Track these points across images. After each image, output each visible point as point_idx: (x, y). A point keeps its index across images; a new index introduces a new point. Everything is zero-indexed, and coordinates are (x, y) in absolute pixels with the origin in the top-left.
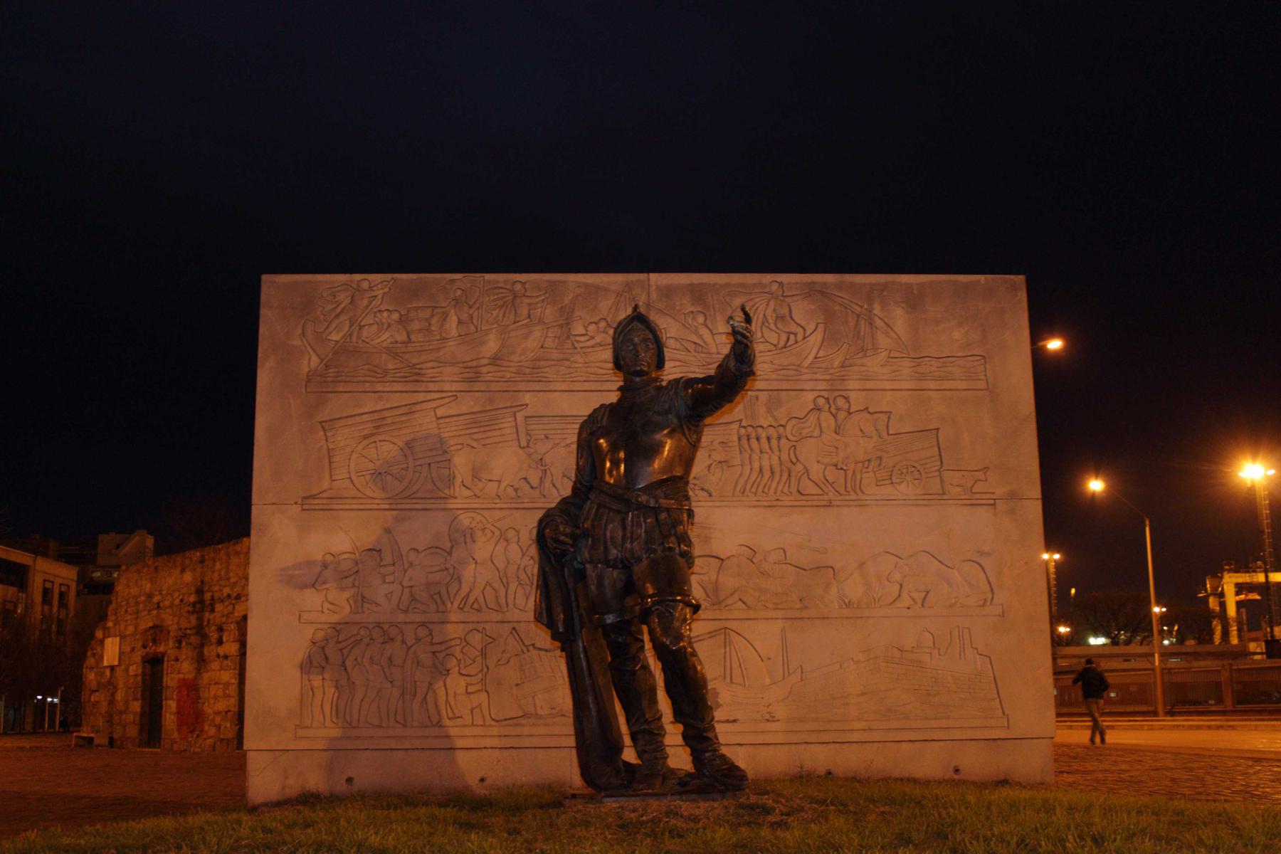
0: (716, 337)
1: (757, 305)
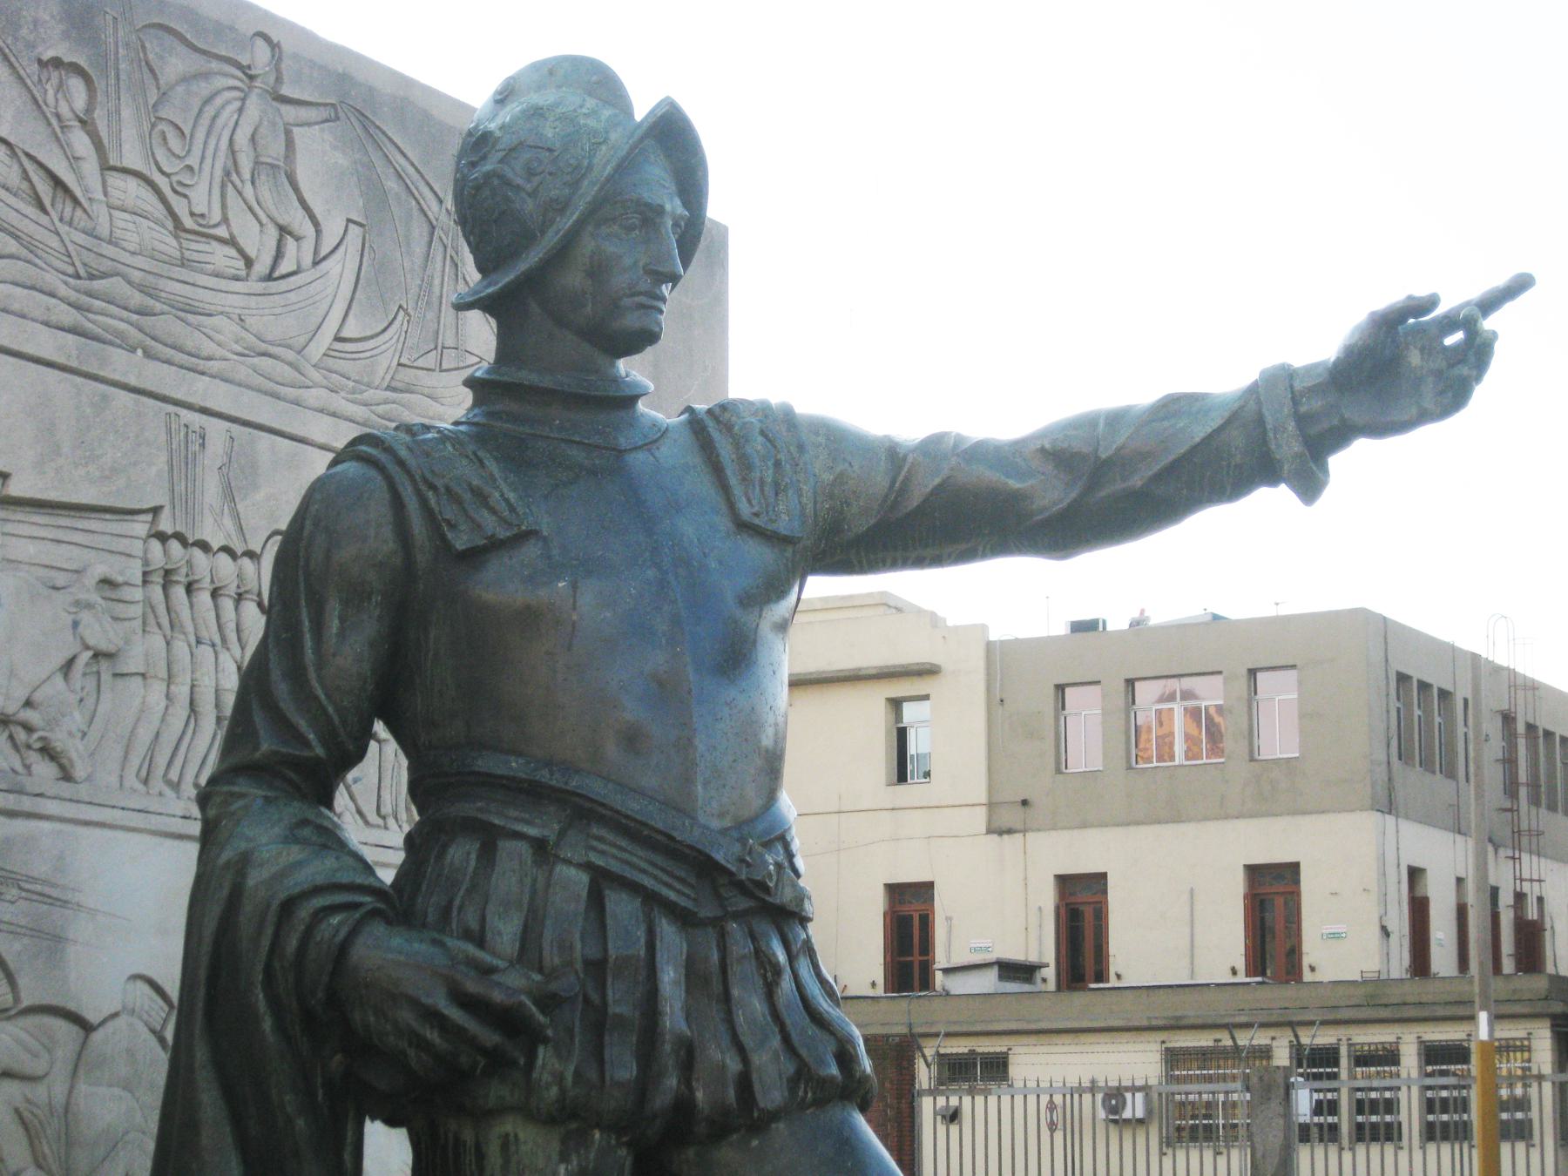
0: (115, 180)
1: (219, 101)
